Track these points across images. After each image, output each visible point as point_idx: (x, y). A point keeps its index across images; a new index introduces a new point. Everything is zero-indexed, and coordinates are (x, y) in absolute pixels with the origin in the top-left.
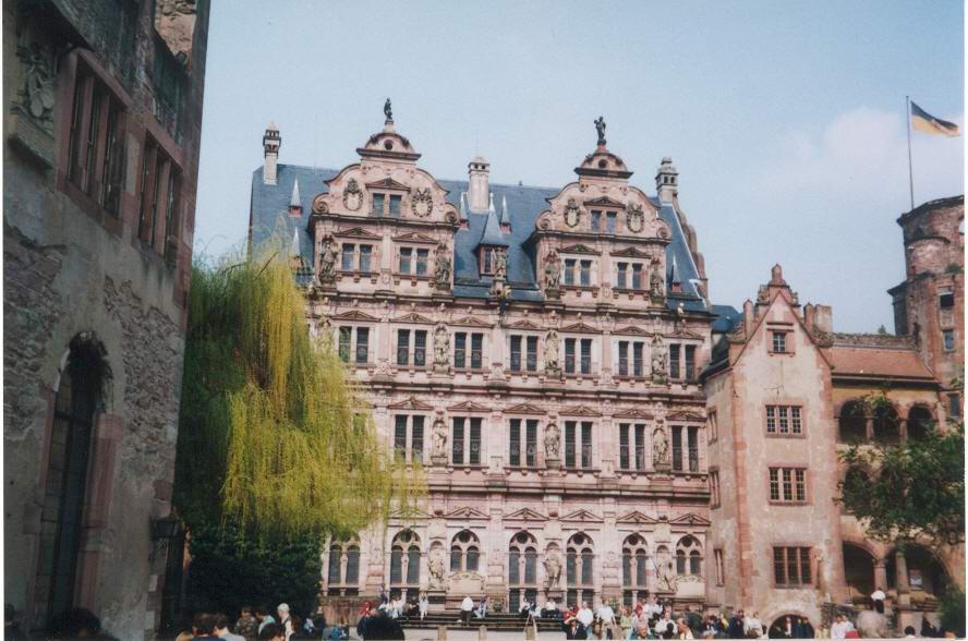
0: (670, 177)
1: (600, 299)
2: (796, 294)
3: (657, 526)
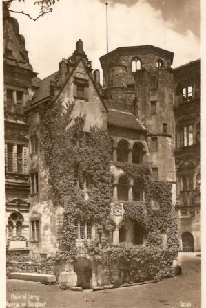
2: (90, 62)
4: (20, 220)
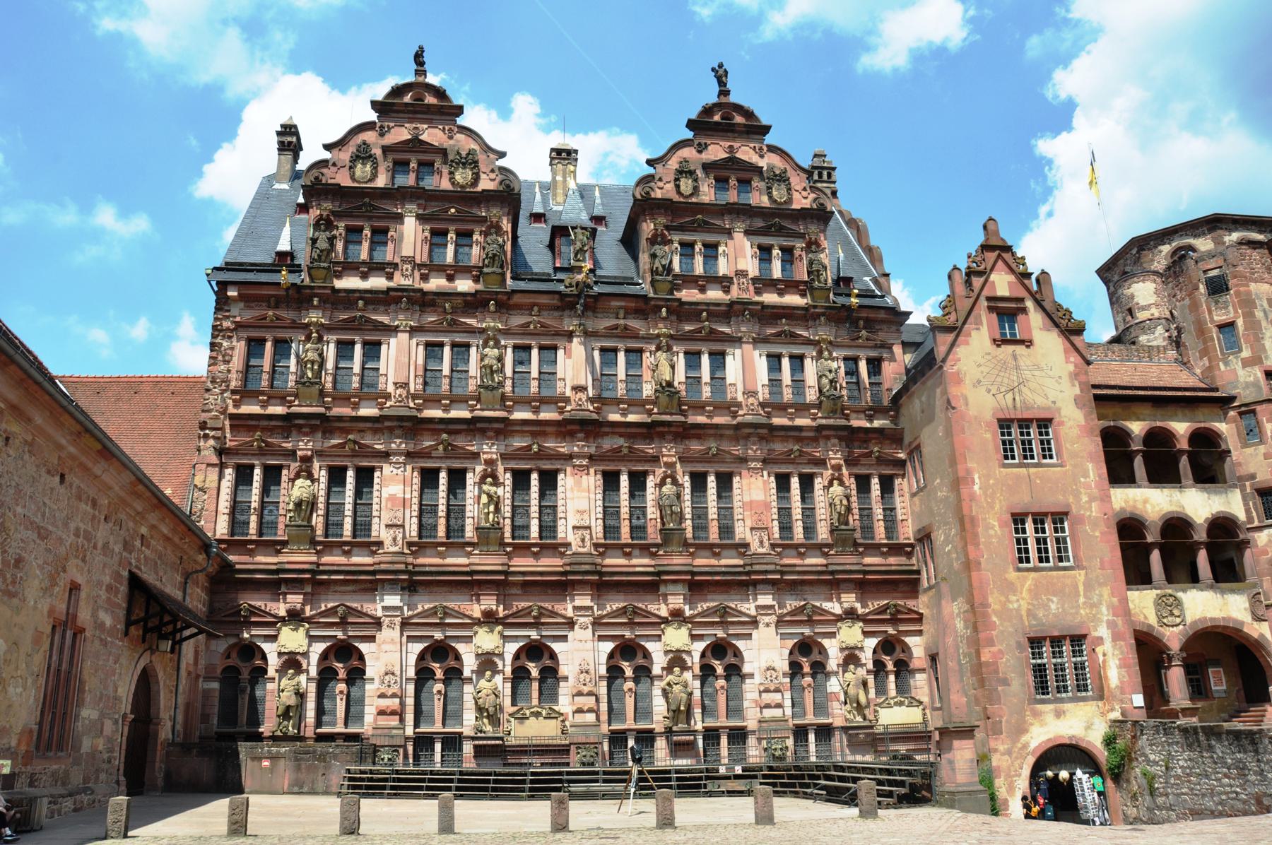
0: (825, 173)
1: (735, 293)
2: (1023, 258)
3: (839, 624)
4: (902, 656)
